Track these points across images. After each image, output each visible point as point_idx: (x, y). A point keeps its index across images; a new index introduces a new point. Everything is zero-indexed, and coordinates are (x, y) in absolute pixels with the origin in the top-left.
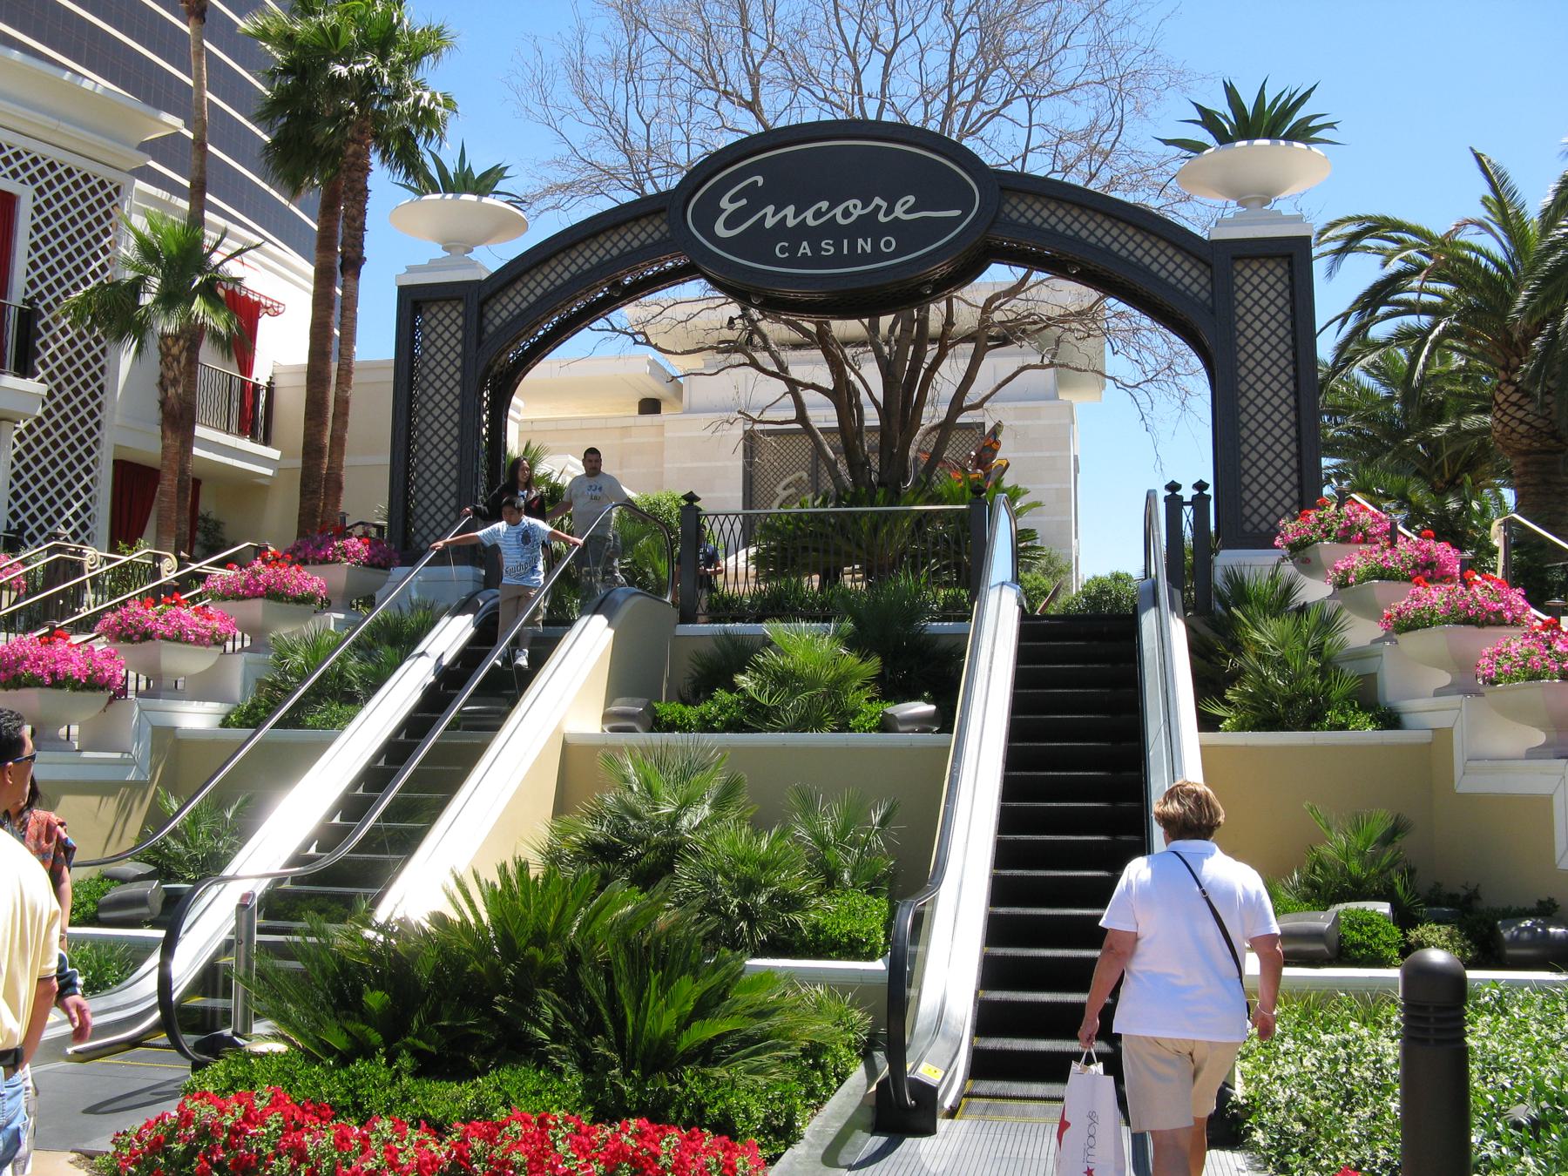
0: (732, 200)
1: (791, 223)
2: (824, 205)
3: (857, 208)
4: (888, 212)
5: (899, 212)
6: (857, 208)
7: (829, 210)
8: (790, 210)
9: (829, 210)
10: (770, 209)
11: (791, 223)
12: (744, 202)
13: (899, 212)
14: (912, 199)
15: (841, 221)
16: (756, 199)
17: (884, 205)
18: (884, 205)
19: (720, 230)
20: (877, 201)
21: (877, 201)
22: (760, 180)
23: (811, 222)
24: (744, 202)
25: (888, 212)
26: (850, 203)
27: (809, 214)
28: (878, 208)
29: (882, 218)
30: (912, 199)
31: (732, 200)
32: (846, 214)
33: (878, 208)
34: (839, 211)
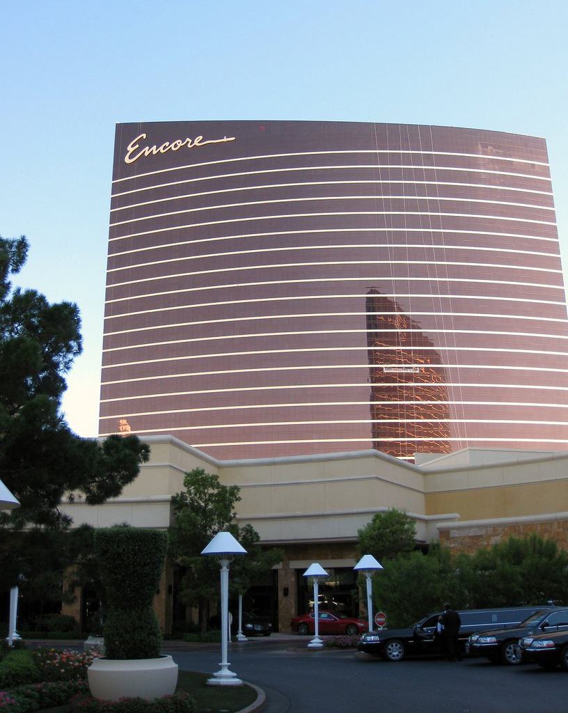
1: (155, 153)
2: (167, 144)
3: (179, 143)
5: (196, 143)
6: (179, 143)
12: (137, 146)
13: (196, 143)
14: (201, 137)
15: (174, 149)
16: (142, 143)
17: (190, 141)
18: (190, 141)
19: (127, 160)
20: (188, 139)
21: (188, 139)
23: (162, 151)
24: (137, 146)
27: (161, 148)
28: (188, 142)
29: (189, 146)
30: (201, 137)
32: (176, 146)
33: (188, 142)
34: (173, 145)
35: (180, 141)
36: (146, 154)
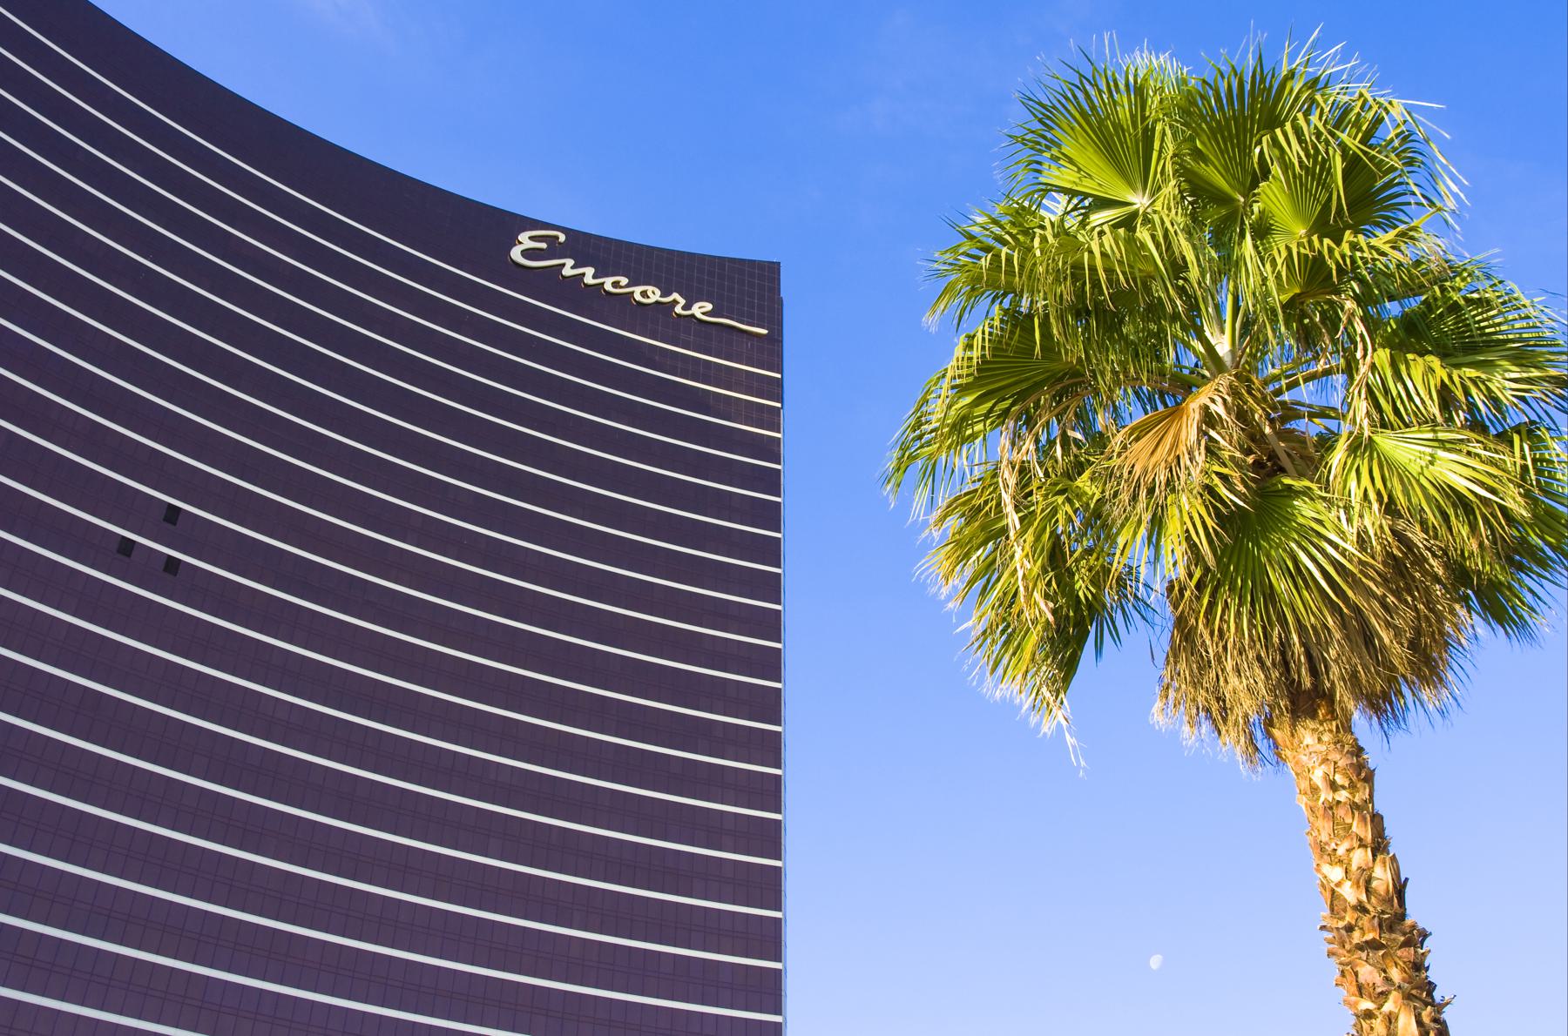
0: (531, 238)
2: (624, 281)
3: (655, 295)
4: (687, 307)
6: (655, 295)
7: (627, 286)
8: (589, 272)
9: (627, 286)
10: (570, 262)
11: (589, 280)
12: (544, 245)
14: (709, 307)
15: (638, 297)
16: (554, 249)
17: (682, 301)
20: (675, 296)
21: (675, 296)
22: (562, 238)
23: (608, 287)
24: (544, 245)
25: (685, 308)
26: (650, 289)
28: (675, 302)
29: (678, 309)
30: (709, 307)
31: (531, 238)
33: (675, 302)
34: (637, 290)
35: (658, 292)
36: (567, 272)
